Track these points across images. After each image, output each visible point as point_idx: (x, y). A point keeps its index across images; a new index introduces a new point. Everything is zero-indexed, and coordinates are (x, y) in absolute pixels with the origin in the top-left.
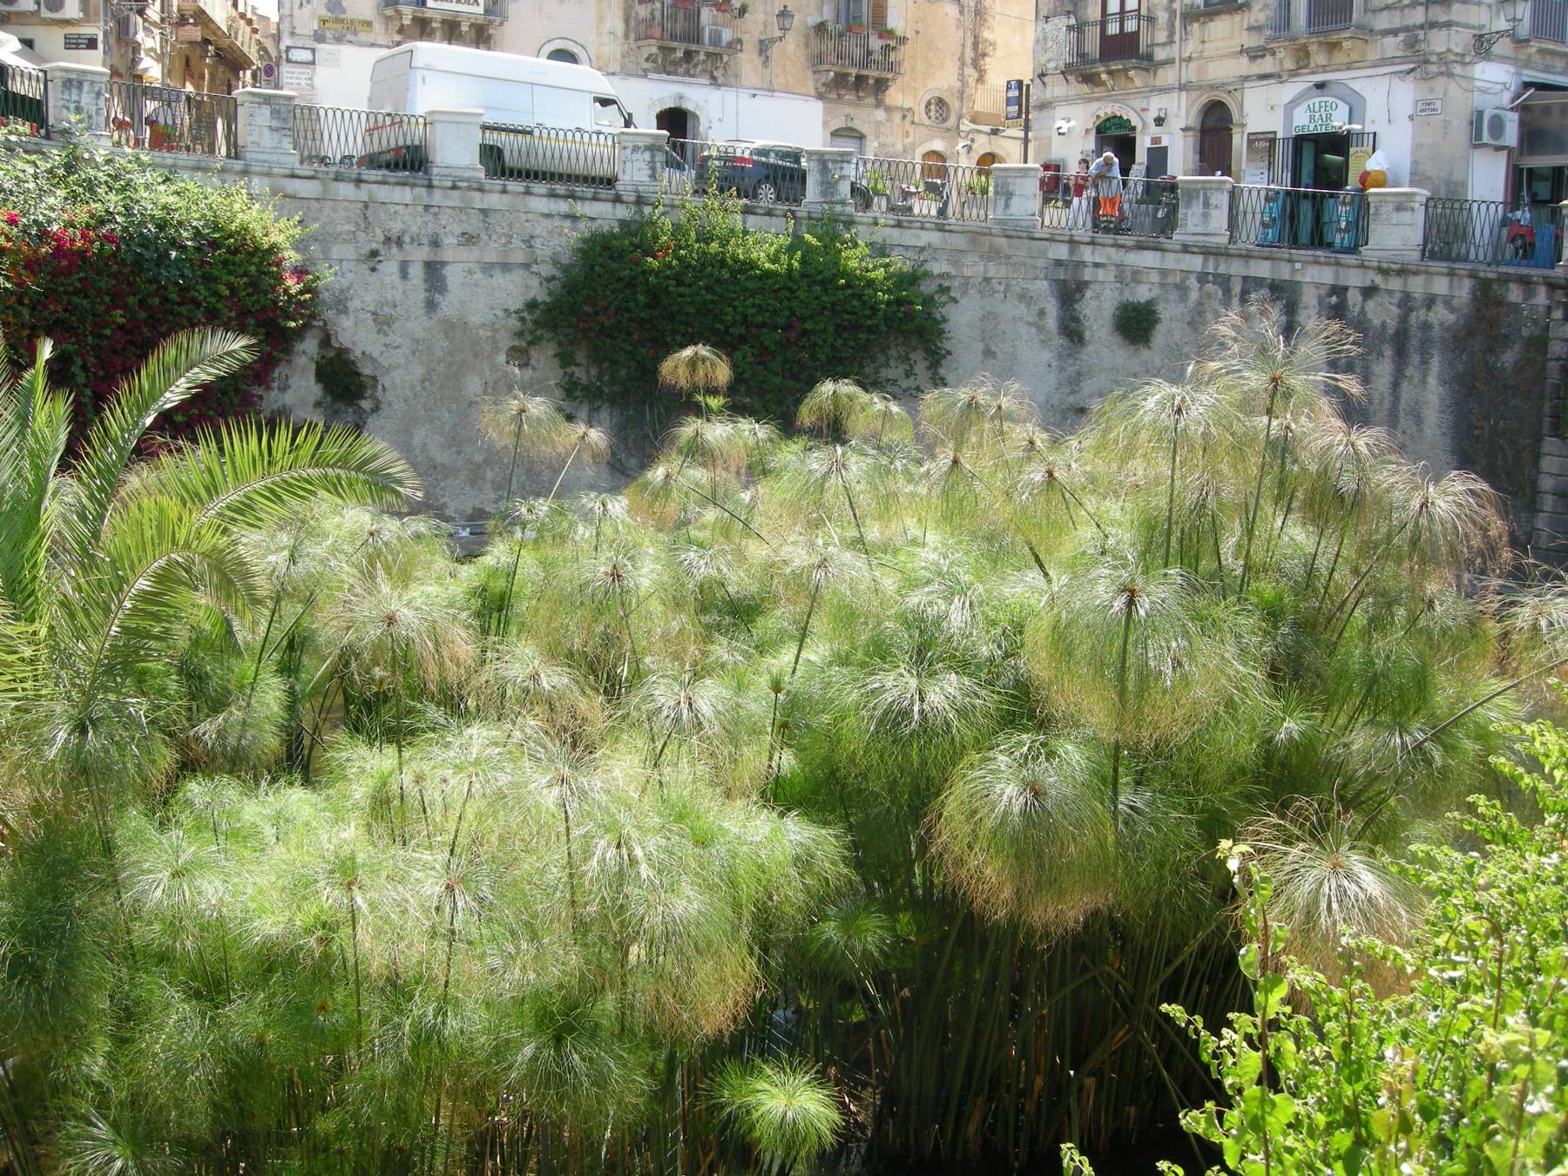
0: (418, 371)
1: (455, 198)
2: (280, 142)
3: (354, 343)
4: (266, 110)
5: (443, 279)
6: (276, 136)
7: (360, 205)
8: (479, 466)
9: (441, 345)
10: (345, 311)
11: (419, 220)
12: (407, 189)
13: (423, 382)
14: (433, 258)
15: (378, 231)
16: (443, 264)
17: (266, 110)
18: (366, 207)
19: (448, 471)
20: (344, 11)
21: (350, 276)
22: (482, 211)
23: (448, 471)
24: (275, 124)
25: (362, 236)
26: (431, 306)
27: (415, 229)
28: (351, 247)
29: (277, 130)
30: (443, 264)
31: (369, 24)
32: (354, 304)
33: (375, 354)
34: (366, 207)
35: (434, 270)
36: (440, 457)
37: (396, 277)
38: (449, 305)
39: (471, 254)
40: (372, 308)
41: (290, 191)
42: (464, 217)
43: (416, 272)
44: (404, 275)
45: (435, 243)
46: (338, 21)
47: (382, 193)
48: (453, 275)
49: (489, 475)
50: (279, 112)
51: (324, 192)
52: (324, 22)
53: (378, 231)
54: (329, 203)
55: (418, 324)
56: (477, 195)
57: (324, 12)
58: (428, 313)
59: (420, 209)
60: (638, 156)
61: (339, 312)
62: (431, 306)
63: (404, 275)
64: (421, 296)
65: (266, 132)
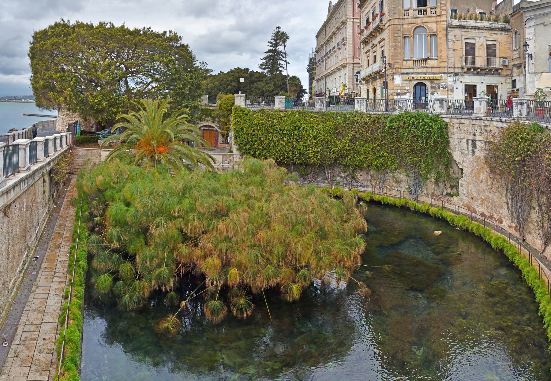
1: (478, 122)
4: (438, 102)
5: (476, 144)
16: (476, 140)
17: (438, 102)
26: (473, 152)
27: (470, 131)
35: (474, 141)
43: (470, 142)
44: (468, 143)
45: (474, 135)
47: (463, 121)
62: (473, 152)
63: (468, 143)
64: (470, 149)
65: (438, 108)
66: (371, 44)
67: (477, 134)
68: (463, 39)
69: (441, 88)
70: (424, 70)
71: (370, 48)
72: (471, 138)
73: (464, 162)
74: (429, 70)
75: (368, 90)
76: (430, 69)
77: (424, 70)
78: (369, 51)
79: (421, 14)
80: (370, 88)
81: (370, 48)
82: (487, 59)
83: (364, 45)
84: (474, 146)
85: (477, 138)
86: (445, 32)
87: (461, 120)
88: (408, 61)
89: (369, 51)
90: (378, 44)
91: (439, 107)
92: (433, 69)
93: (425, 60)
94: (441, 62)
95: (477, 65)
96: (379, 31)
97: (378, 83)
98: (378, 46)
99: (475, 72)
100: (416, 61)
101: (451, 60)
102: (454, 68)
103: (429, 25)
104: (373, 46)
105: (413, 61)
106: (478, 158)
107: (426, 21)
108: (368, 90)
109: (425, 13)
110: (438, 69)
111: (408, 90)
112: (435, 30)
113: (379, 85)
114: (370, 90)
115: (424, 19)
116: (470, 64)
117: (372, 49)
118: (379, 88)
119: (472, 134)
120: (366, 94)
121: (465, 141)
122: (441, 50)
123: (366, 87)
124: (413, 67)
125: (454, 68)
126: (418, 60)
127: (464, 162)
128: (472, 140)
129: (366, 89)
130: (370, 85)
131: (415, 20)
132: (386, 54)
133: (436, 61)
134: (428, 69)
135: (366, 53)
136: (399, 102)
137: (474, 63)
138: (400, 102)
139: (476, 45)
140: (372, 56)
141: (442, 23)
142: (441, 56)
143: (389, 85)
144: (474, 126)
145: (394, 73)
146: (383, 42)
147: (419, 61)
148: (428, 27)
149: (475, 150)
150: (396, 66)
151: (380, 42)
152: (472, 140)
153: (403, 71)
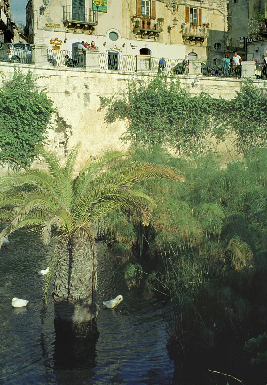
7: (66, 77)
14: (86, 92)
15: (71, 84)
16: (89, 93)
18: (68, 78)
20: (52, 22)
22: (99, 78)
30: (89, 93)
31: (59, 25)
34: (68, 78)
37: (77, 97)
40: (70, 106)
42: (95, 80)
43: (82, 96)
44: (79, 97)
46: (50, 24)
52: (46, 24)
53: (71, 84)
56: (98, 74)
57: (47, 22)
60: (142, 62)
62: (86, 105)
63: (79, 97)
128: (85, 94)
149: (87, 103)
152: (85, 94)
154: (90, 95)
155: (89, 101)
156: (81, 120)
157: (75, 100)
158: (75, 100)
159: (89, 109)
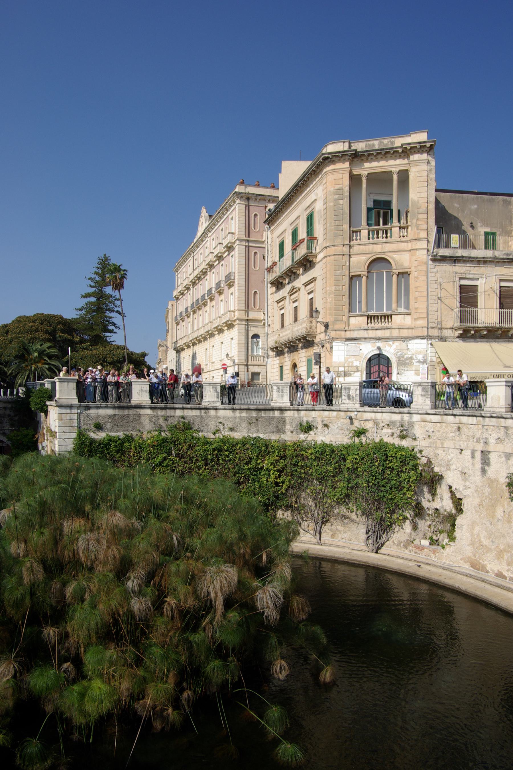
0: (477, 500)
2: (425, 400)
3: (453, 483)
4: (420, 388)
5: (488, 459)
6: (424, 398)
8: (501, 551)
9: (487, 490)
10: (449, 469)
11: (480, 431)
12: (475, 418)
13: (480, 505)
14: (484, 449)
16: (489, 452)
17: (420, 388)
19: (488, 550)
21: (452, 455)
22: (506, 428)
23: (488, 550)
24: (423, 393)
25: (457, 438)
26: (484, 471)
27: (478, 436)
28: (452, 442)
29: (424, 396)
30: (489, 452)
32: (453, 467)
33: (461, 489)
36: (486, 542)
38: (491, 471)
39: (500, 448)
40: (460, 469)
41: (428, 420)
43: (478, 455)
44: (473, 457)
47: (464, 419)
48: (493, 457)
49: (505, 557)
50: (425, 388)
51: (442, 419)
54: (444, 424)
55: (477, 478)
58: (482, 474)
59: (480, 426)
61: (447, 470)
62: (484, 471)
63: (473, 457)
64: (479, 466)
65: (420, 398)
66: (288, 288)
67: (492, 441)
68: (457, 279)
69: (415, 364)
70: (386, 333)
71: (286, 294)
72: (480, 447)
73: (466, 488)
74: (395, 333)
75: (281, 367)
76: (397, 331)
77: (386, 333)
78: (283, 299)
79: (378, 237)
80: (285, 364)
81: (286, 294)
82: (501, 314)
83: (274, 289)
84: (486, 461)
85: (490, 448)
86: (424, 268)
87: (462, 417)
88: (357, 318)
89: (283, 299)
90: (303, 288)
91: (422, 395)
92: (401, 330)
93: (388, 316)
94: (416, 319)
95: (480, 324)
96: (305, 266)
97: (300, 356)
98: (303, 291)
99: (478, 334)
100: (371, 317)
101: (433, 316)
102: (441, 329)
103: (396, 256)
104: (293, 292)
105: (366, 318)
106: (492, 482)
107: (391, 250)
108: (281, 367)
109: (389, 235)
110: (410, 330)
111: (357, 367)
112: (406, 264)
113: (305, 359)
114: (285, 368)
115: (388, 245)
116: (468, 321)
117: (291, 295)
118: (305, 364)
119: (482, 441)
120: (278, 374)
121: (467, 453)
122: (416, 298)
123: (278, 362)
124: (366, 327)
125: (441, 329)
126: (374, 316)
127: (466, 488)
128: (482, 452)
129: (278, 366)
130: (287, 359)
131: (371, 247)
132: (317, 305)
133: (408, 318)
134: (393, 331)
135: (278, 302)
136: (349, 389)
137: (476, 320)
138: (352, 388)
139: (480, 289)
140: (289, 307)
141: (418, 252)
142: (416, 309)
143: (322, 360)
144: (486, 427)
145: (333, 339)
146: (312, 284)
147: (378, 316)
148: (394, 260)
149: (487, 468)
150: (336, 327)
151: (306, 285)
152: (482, 452)
153: (349, 335)
154: (491, 454)
155: (488, 464)
156: (475, 494)
157: (468, 461)
158: (468, 461)
159: (490, 479)
